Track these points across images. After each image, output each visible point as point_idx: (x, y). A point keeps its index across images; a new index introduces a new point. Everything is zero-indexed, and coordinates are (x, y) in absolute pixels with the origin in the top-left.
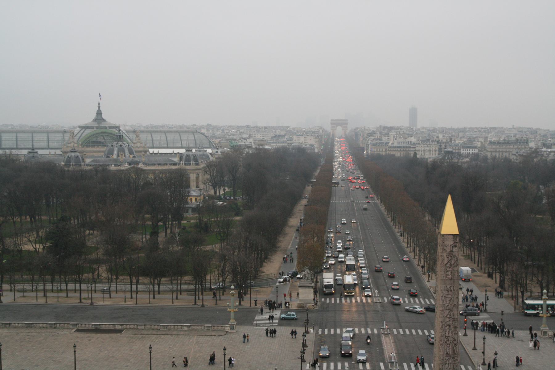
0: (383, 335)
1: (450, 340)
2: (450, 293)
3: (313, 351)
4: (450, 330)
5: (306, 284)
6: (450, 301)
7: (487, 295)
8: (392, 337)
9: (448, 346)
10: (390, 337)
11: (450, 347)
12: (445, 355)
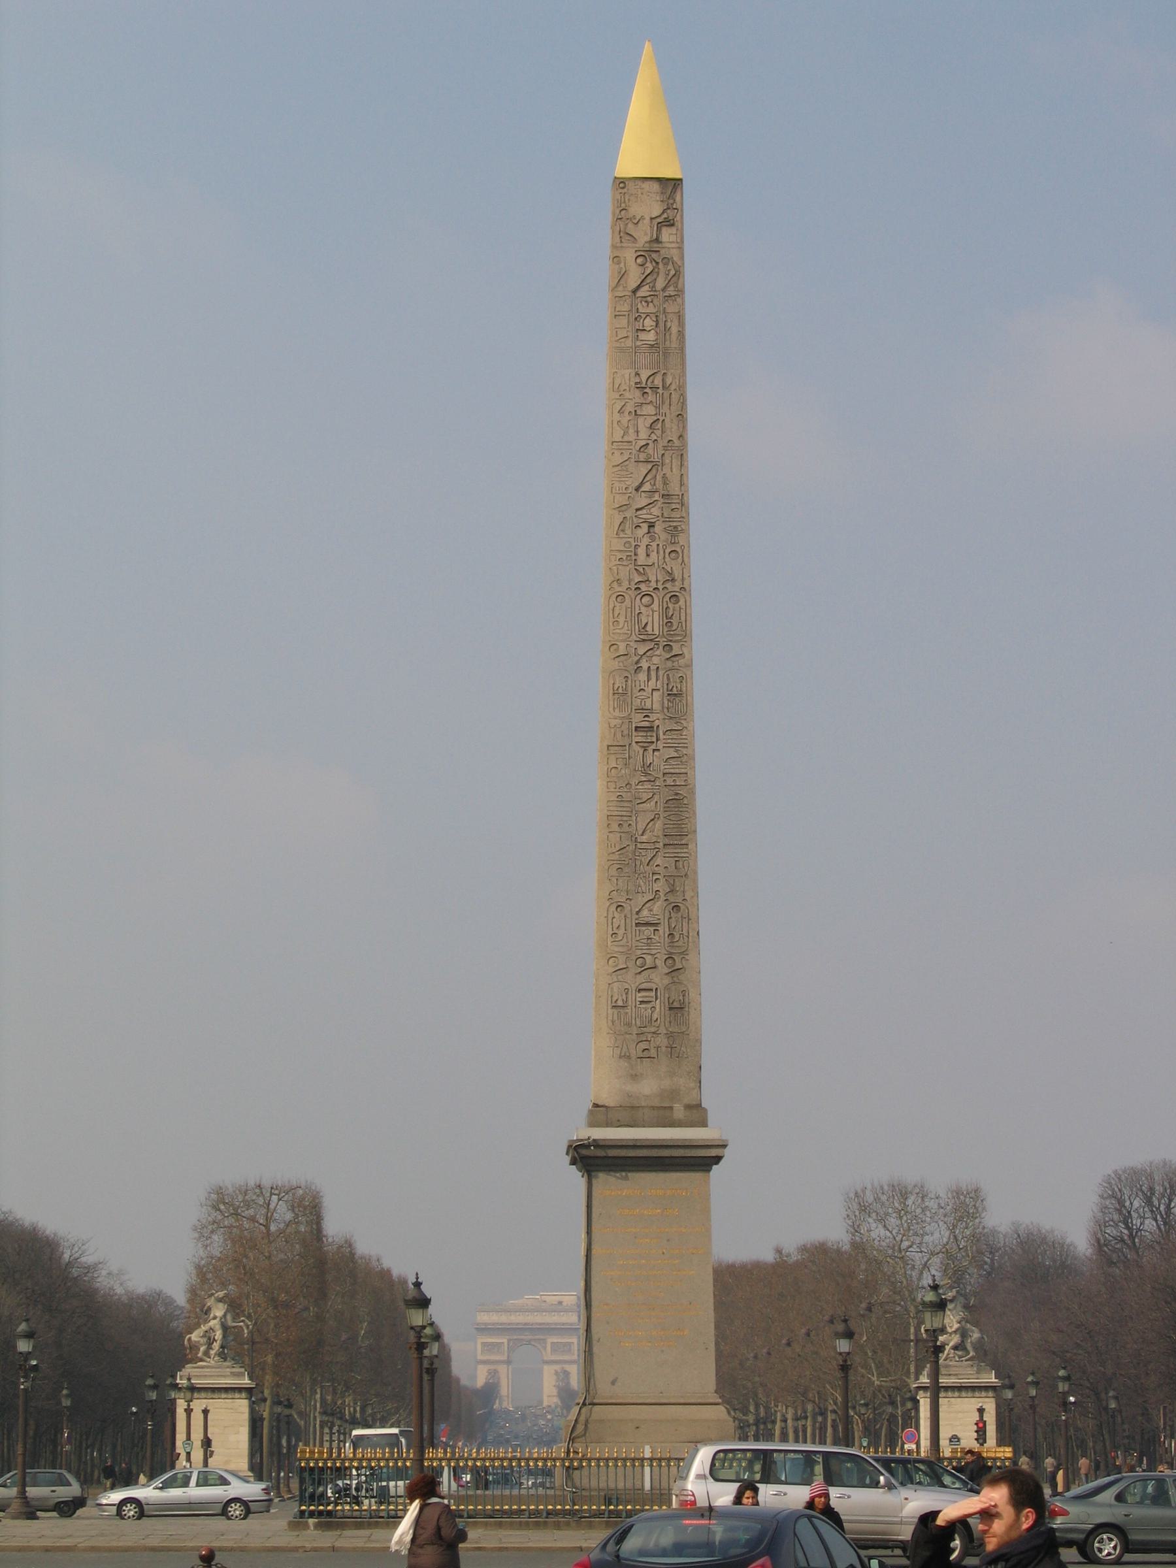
1: (653, 578)
2: (650, 398)
11: (655, 606)
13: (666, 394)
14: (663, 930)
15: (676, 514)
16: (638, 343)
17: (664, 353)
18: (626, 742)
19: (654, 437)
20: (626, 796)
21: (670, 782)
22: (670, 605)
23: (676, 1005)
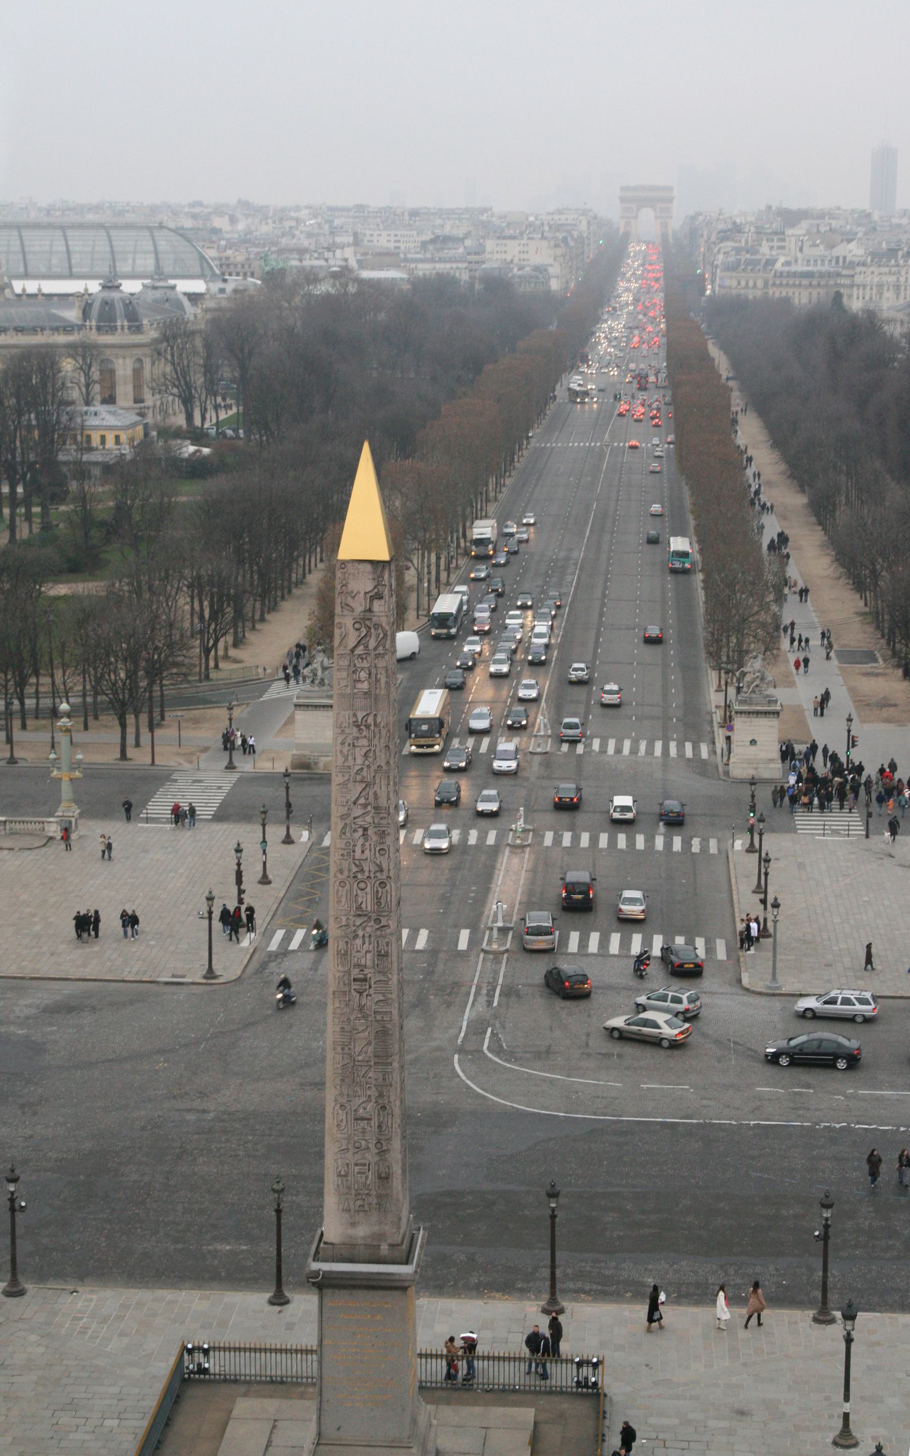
0: (508, 849)
1: (366, 869)
2: (364, 733)
3: (281, 895)
4: (366, 840)
5: (315, 698)
6: (366, 755)
7: (852, 733)
8: (533, 856)
9: (362, 885)
10: (527, 856)
11: (368, 890)
12: (352, 913)
13: (377, 730)
14: (375, 1123)
15: (384, 822)
16: (355, 691)
17: (375, 699)
18: (346, 989)
19: (367, 763)
20: (347, 1028)
21: (379, 1017)
22: (380, 890)
23: (383, 1175)
